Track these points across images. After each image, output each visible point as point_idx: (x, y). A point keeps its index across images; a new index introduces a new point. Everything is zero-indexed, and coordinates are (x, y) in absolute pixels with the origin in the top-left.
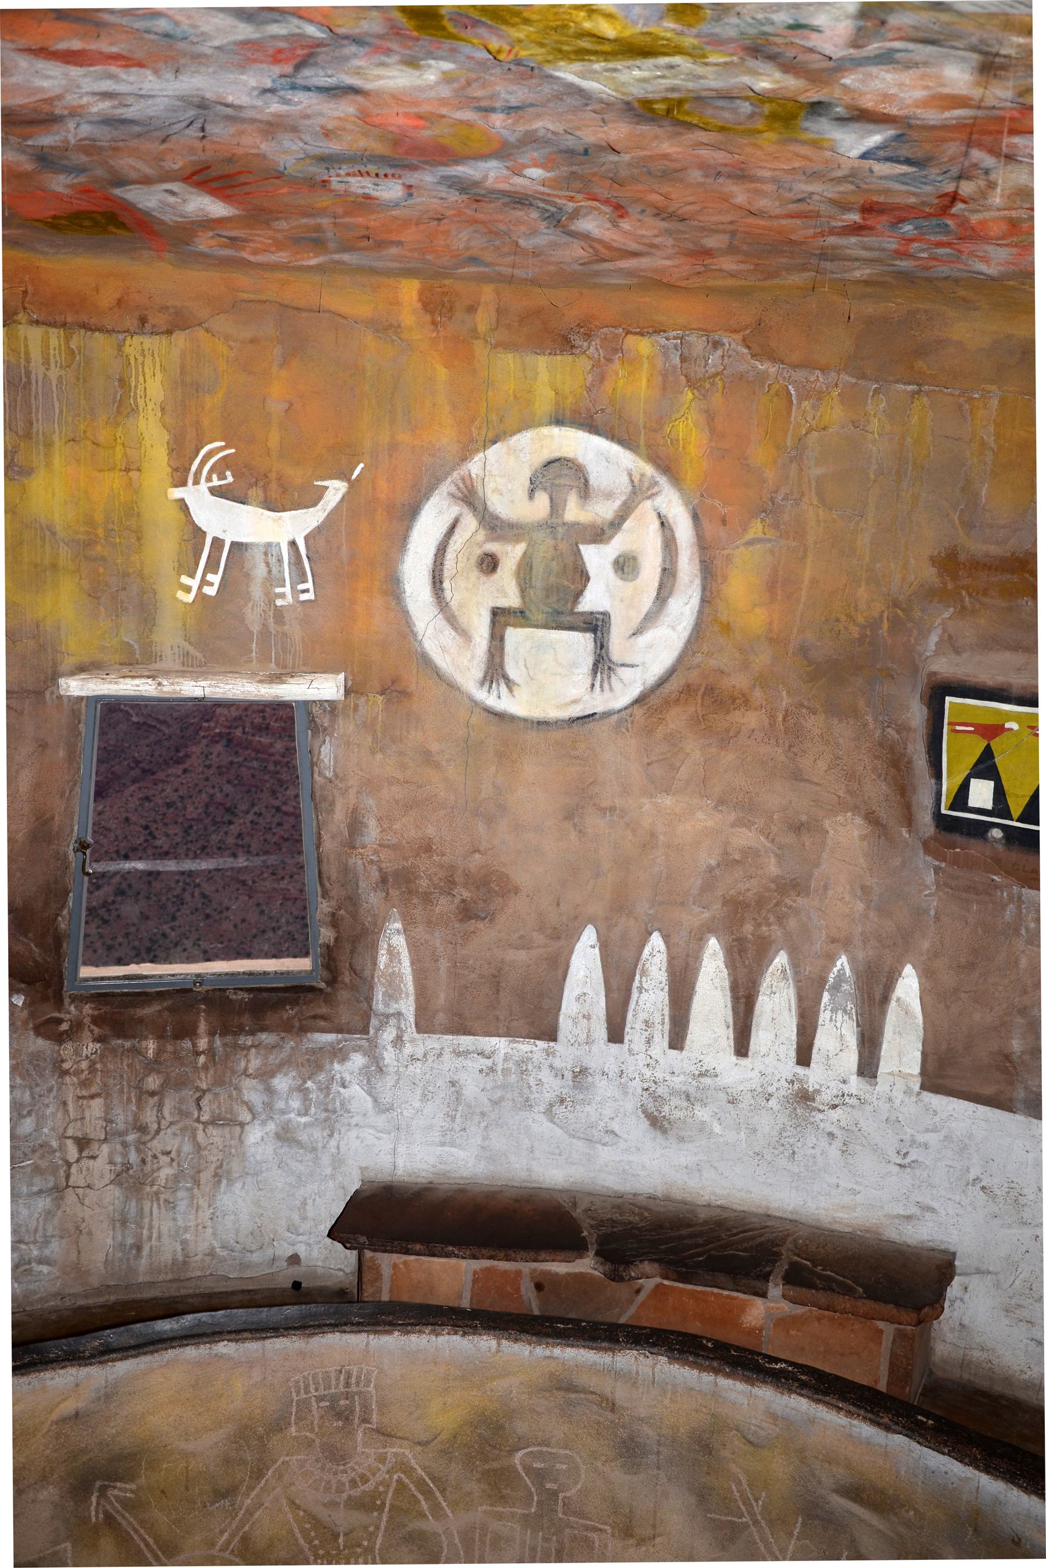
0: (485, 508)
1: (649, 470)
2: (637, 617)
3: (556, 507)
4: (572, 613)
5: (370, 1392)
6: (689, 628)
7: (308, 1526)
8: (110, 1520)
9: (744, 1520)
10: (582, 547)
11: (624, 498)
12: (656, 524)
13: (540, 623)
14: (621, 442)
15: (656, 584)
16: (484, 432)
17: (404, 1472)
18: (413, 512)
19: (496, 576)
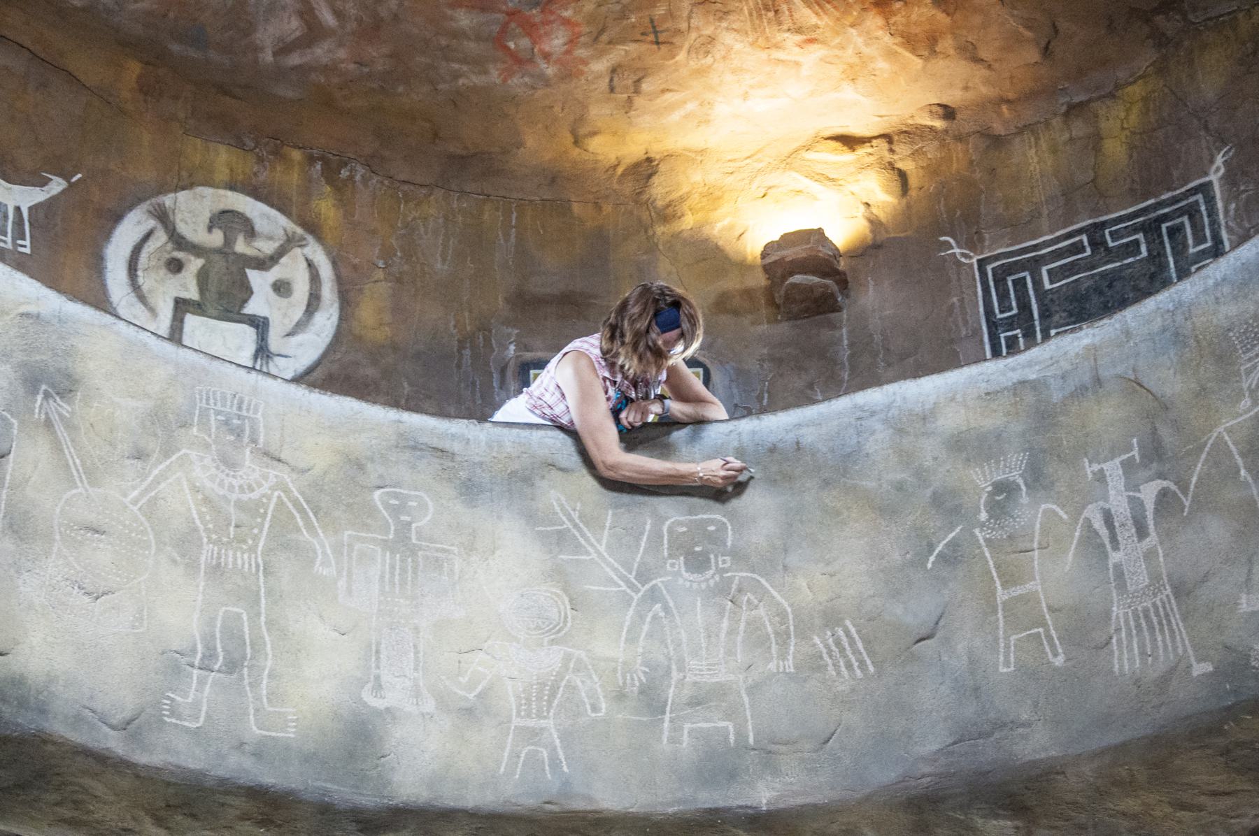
0: (174, 229)
1: (299, 231)
2: (289, 325)
3: (229, 242)
4: (239, 313)
5: (257, 419)
6: (331, 336)
7: (204, 510)
8: (48, 424)
9: (565, 526)
10: (248, 271)
11: (282, 242)
12: (304, 265)
13: (214, 315)
14: (280, 210)
15: (305, 302)
16: (175, 181)
17: (285, 492)
18: (118, 218)
19: (180, 276)
